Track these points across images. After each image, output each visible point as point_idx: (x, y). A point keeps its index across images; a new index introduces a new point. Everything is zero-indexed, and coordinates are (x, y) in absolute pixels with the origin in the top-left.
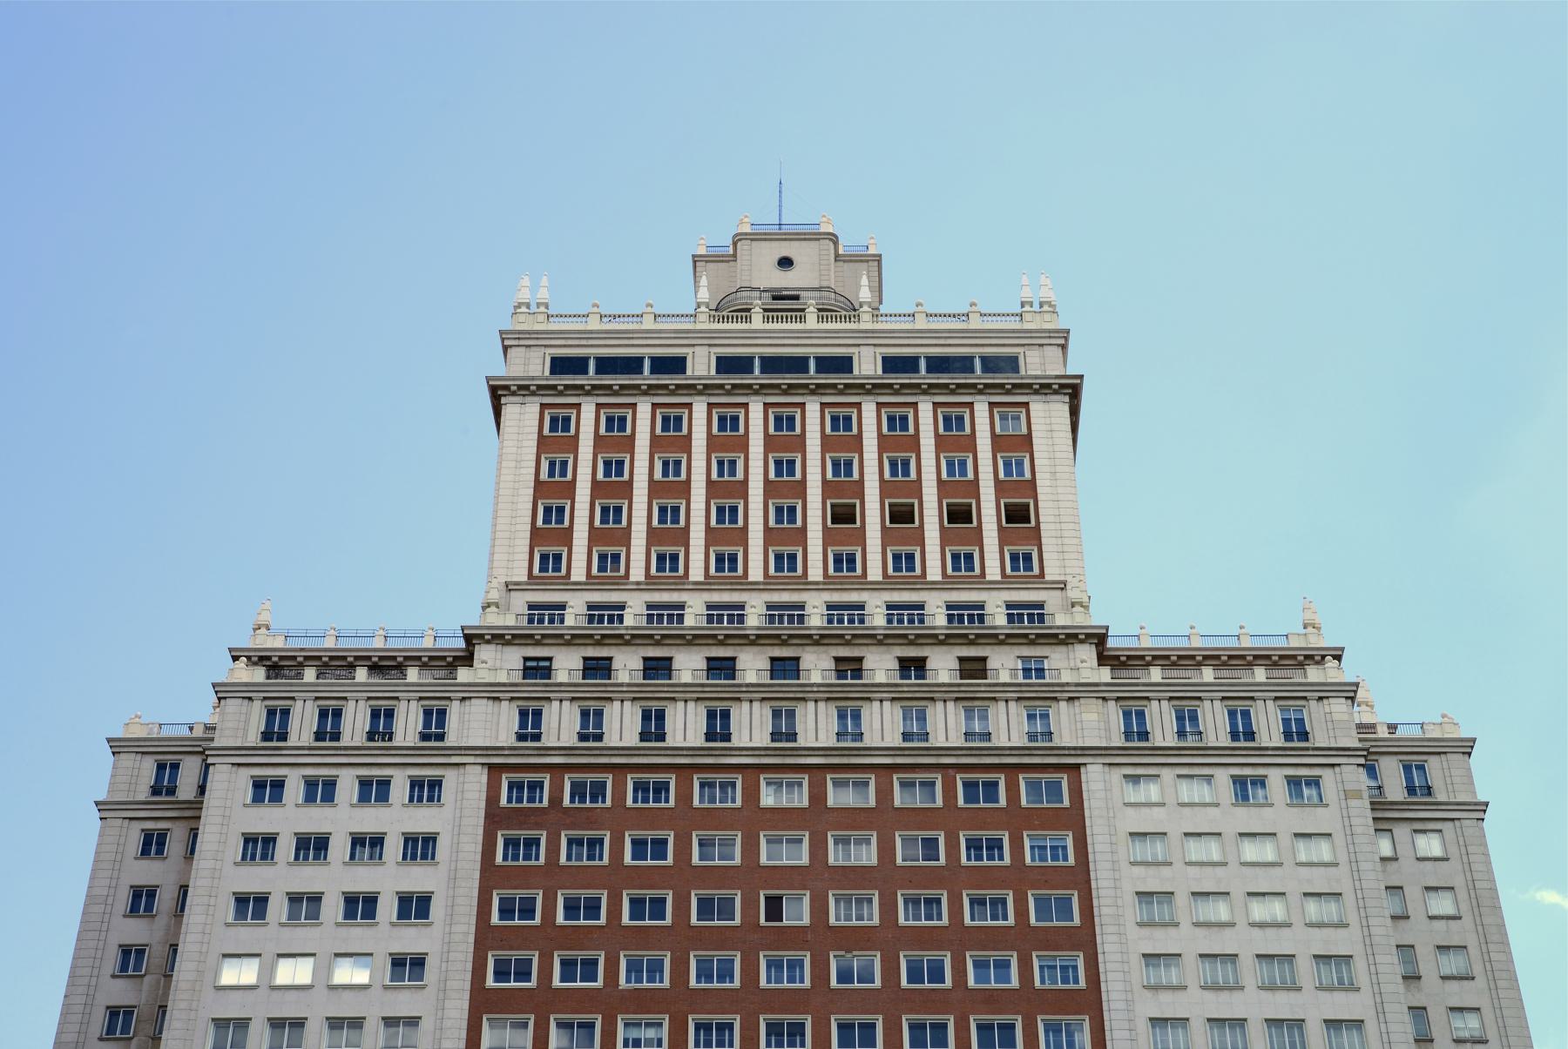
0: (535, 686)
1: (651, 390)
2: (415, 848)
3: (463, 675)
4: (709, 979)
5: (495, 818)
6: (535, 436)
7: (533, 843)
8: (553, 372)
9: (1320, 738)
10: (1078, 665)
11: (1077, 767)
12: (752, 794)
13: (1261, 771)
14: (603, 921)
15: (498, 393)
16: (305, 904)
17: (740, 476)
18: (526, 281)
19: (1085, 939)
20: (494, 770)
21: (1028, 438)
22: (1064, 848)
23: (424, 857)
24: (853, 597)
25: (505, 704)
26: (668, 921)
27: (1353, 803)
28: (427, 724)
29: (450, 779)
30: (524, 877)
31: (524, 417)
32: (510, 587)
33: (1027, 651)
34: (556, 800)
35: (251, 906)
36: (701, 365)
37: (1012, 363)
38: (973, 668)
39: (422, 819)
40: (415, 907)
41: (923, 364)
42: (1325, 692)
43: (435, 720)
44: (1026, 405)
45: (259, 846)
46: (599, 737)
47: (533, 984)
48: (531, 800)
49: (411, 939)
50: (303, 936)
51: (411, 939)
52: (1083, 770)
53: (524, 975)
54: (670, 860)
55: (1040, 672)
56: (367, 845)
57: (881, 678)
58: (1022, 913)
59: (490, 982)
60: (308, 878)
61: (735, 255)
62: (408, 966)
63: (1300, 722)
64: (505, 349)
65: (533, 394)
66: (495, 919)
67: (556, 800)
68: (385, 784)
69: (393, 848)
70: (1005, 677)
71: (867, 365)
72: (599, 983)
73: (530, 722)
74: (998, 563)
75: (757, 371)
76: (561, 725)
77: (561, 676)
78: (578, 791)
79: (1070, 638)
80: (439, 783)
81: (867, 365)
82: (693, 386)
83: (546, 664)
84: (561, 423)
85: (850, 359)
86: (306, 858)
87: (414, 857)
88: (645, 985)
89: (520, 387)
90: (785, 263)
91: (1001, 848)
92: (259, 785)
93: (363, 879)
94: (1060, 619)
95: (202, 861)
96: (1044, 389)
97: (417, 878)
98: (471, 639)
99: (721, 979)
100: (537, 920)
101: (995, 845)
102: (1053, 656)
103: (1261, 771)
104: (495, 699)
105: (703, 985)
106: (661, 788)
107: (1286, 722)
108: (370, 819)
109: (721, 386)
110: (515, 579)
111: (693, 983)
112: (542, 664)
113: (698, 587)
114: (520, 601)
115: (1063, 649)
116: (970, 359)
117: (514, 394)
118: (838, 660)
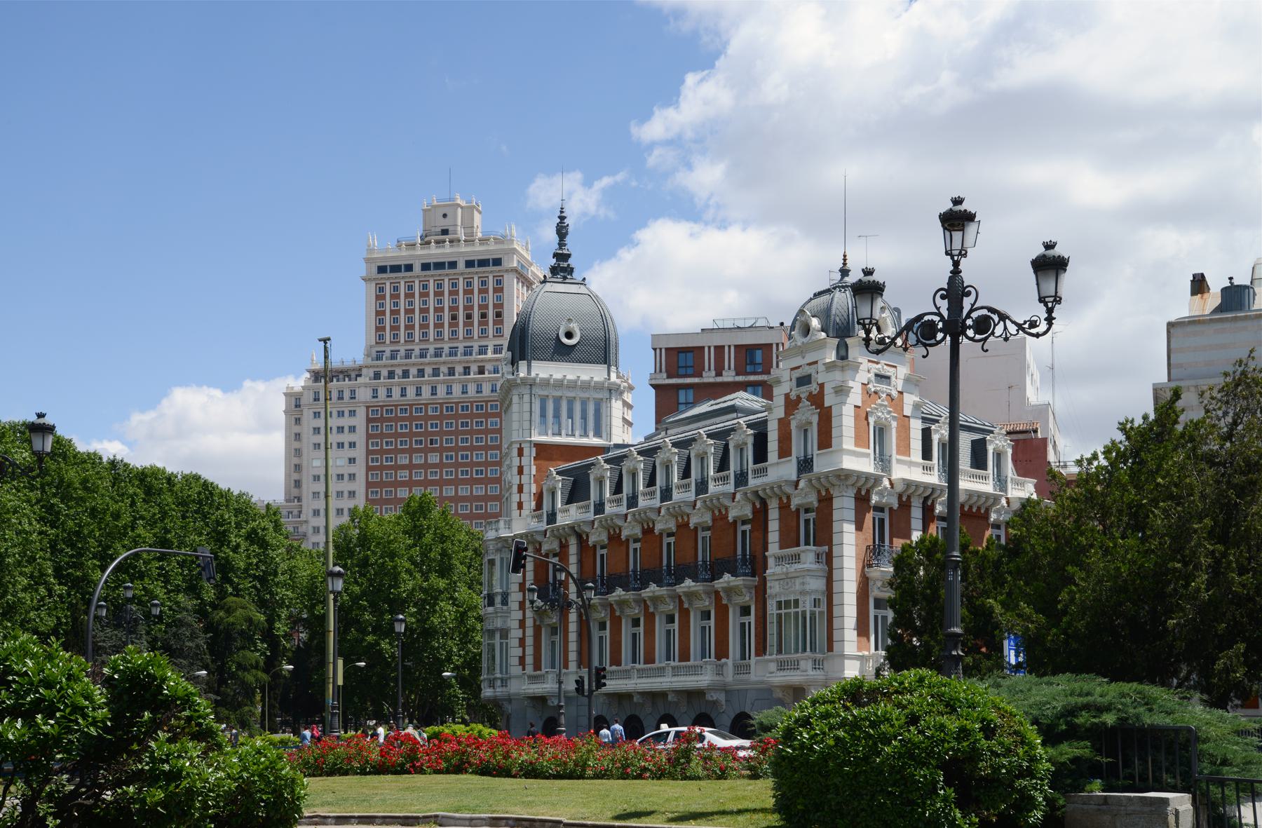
5: (369, 420)
20: (368, 407)
24: (455, 345)
29: (358, 410)
33: (495, 363)
34: (382, 415)
40: (352, 445)
43: (353, 392)
44: (503, 276)
62: (352, 461)
67: (382, 415)
68: (343, 412)
76: (382, 393)
84: (381, 290)
90: (445, 216)
92: (315, 413)
96: (507, 271)
106: (406, 409)
113: (417, 344)
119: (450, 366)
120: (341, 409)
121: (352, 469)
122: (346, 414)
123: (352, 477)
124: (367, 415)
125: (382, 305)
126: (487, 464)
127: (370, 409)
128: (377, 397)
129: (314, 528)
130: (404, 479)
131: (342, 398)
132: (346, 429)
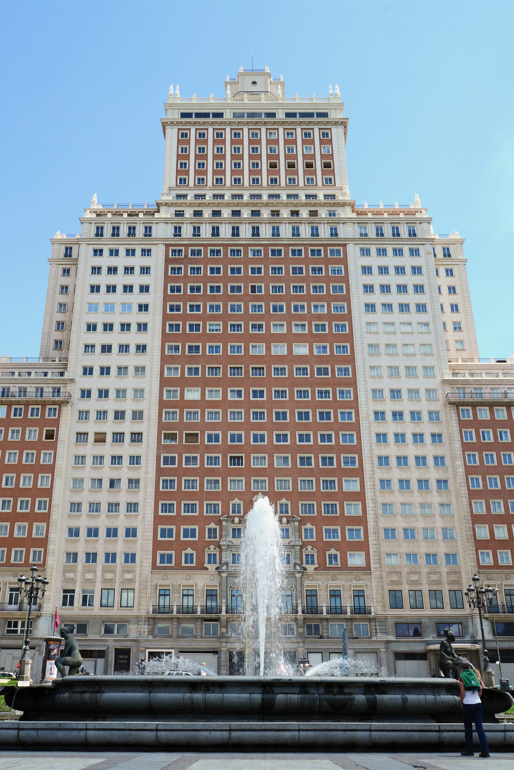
0: (179, 219)
1: (212, 123)
2: (144, 271)
3: (157, 215)
4: (234, 311)
5: (168, 261)
6: (177, 139)
7: (179, 269)
8: (181, 117)
9: (419, 235)
10: (347, 213)
11: (345, 245)
12: (246, 253)
13: (401, 246)
14: (202, 293)
15: (164, 125)
16: (111, 289)
17: (241, 153)
18: (172, 87)
19: (347, 299)
20: (167, 246)
21: (331, 140)
22: (341, 270)
23: (147, 273)
25: (170, 225)
26: (221, 293)
27: (429, 256)
28: (146, 231)
29: (154, 249)
30: (177, 279)
31: (173, 133)
32: (170, 189)
34: (186, 255)
35: (95, 289)
36: (228, 115)
37: (325, 115)
38: (313, 213)
39: (146, 261)
40: (145, 289)
41: (298, 115)
42: (421, 221)
44: (330, 129)
45: (96, 270)
46: (199, 235)
47: (181, 312)
48: (179, 255)
49: (144, 299)
50: (111, 298)
51: (144, 299)
52: (347, 245)
53: (178, 309)
54: (221, 274)
55: (334, 215)
56: (129, 270)
57: (285, 216)
58: (328, 290)
59: (168, 312)
60: (112, 280)
61: (238, 82)
63: (414, 231)
64: (166, 110)
65: (175, 125)
66: (169, 292)
67: (186, 255)
69: (137, 270)
70: (323, 216)
71: (281, 115)
72: (201, 312)
73: (178, 231)
74: (321, 181)
75: (246, 117)
76: (187, 231)
77: (187, 215)
78: (193, 252)
79: (343, 204)
80: (150, 250)
81: (281, 115)
82: (225, 122)
83: (182, 213)
85: (275, 113)
86: (111, 273)
87: (144, 273)
88: (215, 313)
89: (171, 123)
90: (254, 83)
91: (322, 271)
92: (95, 251)
93: (129, 280)
94: (340, 198)
95: (80, 275)
96: (336, 123)
97: (145, 280)
98: (158, 205)
99: (238, 311)
100: (182, 293)
101: (320, 269)
102: (338, 210)
103: (401, 246)
104: (166, 223)
105: (232, 313)
106: (218, 252)
107: (409, 231)
108: (130, 261)
109: (235, 122)
110: (172, 186)
111: (229, 312)
112: (181, 213)
113: (229, 189)
114: (174, 193)
115: (341, 208)
116: (313, 113)
117: (169, 125)
118: (272, 211)
119: (274, 209)
120: (131, 247)
121: (143, 318)
122: (138, 252)
123: (143, 327)
124: (167, 255)
125: (184, 150)
126: (330, 317)
127: (171, 248)
128: (180, 235)
129: (83, 392)
130: (218, 332)
131: (134, 235)
132: (137, 270)
